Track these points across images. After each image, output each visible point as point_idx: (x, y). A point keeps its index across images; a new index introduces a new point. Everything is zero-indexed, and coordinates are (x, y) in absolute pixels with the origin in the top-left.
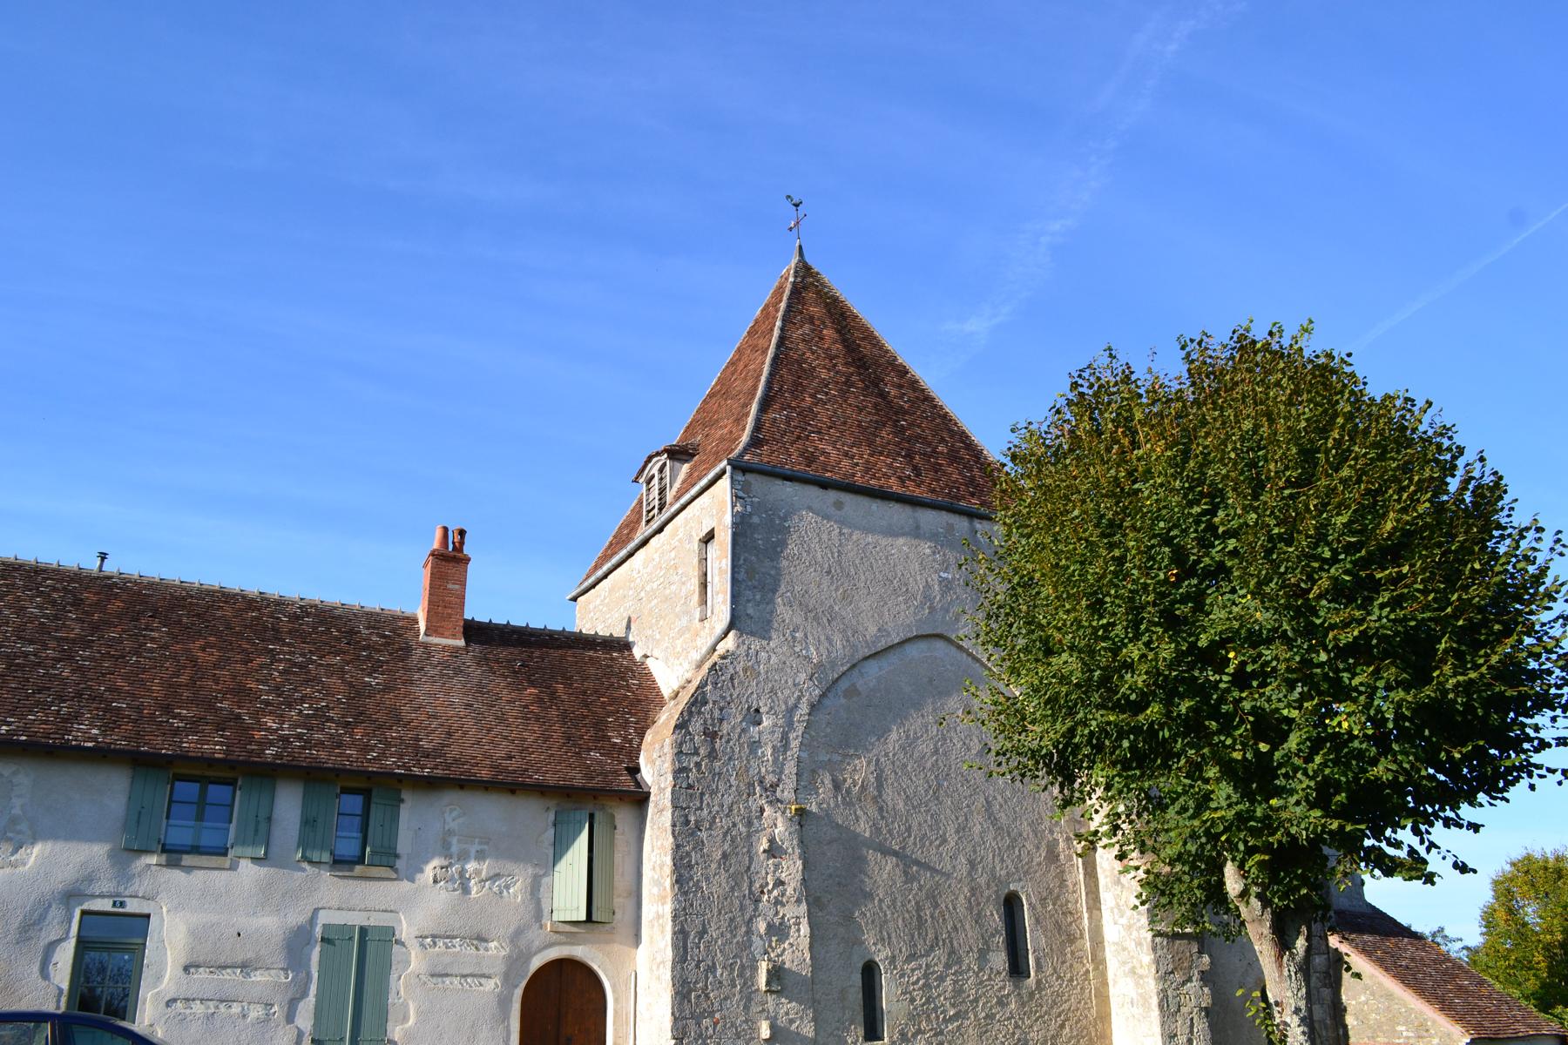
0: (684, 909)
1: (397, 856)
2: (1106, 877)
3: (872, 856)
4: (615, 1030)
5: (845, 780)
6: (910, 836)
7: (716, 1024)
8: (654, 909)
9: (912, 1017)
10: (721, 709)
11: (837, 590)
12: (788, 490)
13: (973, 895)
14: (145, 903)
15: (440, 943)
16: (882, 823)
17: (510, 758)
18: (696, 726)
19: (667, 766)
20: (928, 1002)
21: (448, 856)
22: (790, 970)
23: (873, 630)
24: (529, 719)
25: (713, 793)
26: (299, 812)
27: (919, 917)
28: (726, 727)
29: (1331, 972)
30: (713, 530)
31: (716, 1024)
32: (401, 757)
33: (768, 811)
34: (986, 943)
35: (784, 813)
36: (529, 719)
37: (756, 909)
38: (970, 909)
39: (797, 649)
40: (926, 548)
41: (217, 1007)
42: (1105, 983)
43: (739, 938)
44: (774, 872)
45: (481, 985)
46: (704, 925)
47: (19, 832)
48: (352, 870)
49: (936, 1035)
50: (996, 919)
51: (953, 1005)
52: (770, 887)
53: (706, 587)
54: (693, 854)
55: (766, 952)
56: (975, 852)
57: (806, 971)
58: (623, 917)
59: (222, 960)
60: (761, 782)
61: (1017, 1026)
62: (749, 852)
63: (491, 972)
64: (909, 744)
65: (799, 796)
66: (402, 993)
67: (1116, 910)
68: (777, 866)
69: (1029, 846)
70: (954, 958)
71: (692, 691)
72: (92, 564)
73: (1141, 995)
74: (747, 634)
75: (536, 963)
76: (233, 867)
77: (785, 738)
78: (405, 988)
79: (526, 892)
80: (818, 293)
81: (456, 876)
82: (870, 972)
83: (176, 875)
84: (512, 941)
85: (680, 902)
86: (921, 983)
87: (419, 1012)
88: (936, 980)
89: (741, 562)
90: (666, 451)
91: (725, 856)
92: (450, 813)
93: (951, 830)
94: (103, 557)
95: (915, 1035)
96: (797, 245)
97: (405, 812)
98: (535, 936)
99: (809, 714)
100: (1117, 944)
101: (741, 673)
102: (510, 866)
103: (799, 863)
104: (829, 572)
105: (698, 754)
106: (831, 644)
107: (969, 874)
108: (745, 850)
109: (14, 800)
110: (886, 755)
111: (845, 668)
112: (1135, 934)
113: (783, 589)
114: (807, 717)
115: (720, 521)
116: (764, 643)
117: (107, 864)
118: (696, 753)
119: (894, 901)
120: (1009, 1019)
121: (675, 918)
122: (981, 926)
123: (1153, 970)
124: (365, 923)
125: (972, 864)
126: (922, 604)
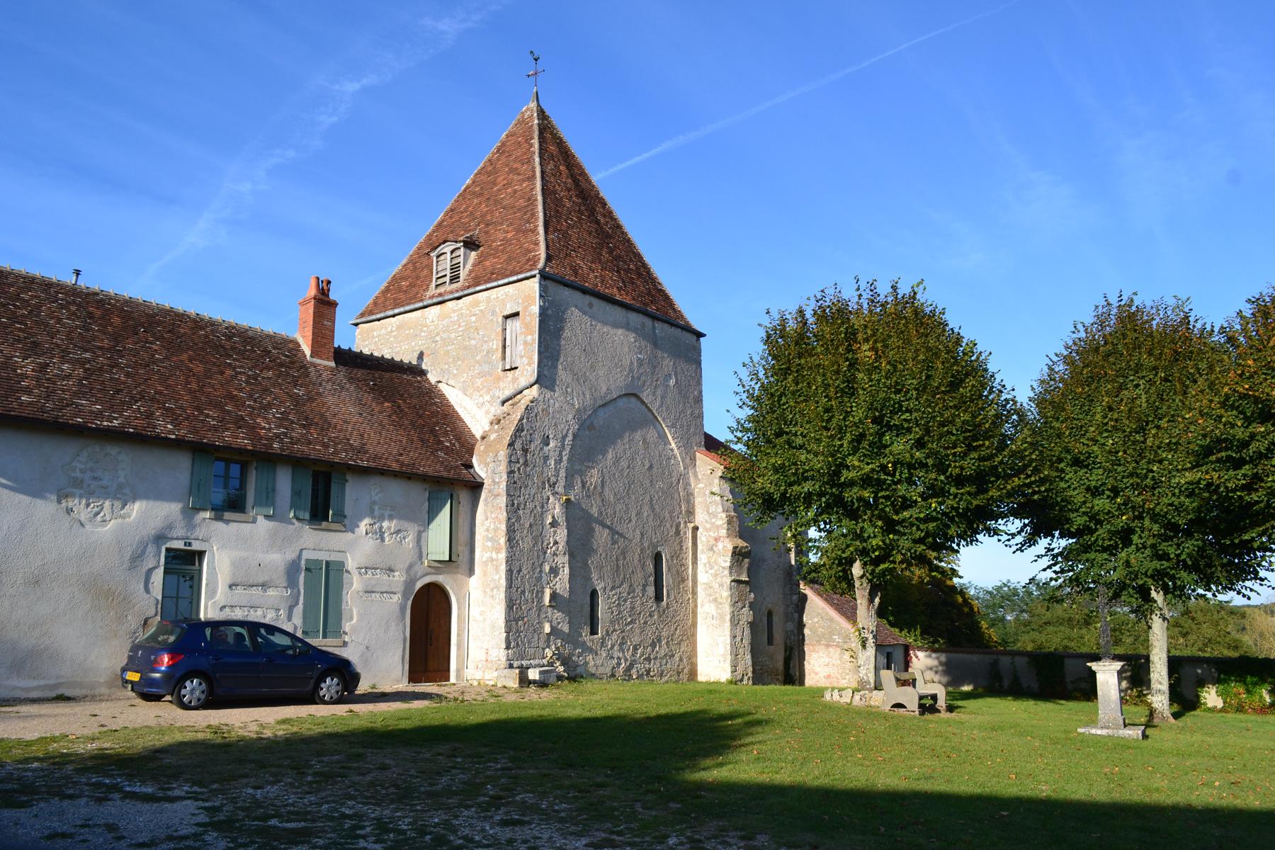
1: (345, 517)
3: (598, 528)
4: (458, 626)
7: (525, 624)
8: (488, 554)
9: (612, 622)
10: (531, 435)
11: (588, 362)
12: (566, 292)
14: (204, 543)
15: (369, 572)
16: (603, 509)
17: (401, 455)
18: (518, 445)
19: (503, 468)
20: (619, 614)
21: (373, 517)
22: (558, 594)
23: (604, 389)
25: (526, 486)
26: (290, 486)
27: (617, 565)
31: (525, 624)
32: (346, 451)
33: (551, 498)
34: (646, 581)
37: (544, 558)
38: (640, 561)
41: (249, 611)
42: (696, 606)
47: (125, 494)
48: (320, 525)
49: (622, 632)
50: (650, 568)
51: (630, 616)
55: (548, 583)
57: (566, 595)
58: (463, 558)
59: (251, 582)
61: (657, 629)
64: (617, 461)
66: (349, 603)
68: (555, 532)
69: (668, 526)
70: (631, 590)
71: (516, 422)
72: (70, 279)
73: (719, 613)
75: (419, 585)
76: (254, 521)
77: (560, 454)
82: (594, 594)
83: (220, 525)
87: (359, 615)
91: (531, 525)
93: (634, 515)
94: (78, 273)
95: (612, 632)
96: (535, 91)
97: (349, 488)
102: (405, 524)
103: (566, 531)
104: (585, 350)
107: (641, 541)
109: (119, 472)
112: (719, 580)
113: (561, 360)
116: (552, 393)
117: (180, 517)
118: (518, 462)
119: (607, 555)
120: (653, 624)
121: (507, 561)
122: (644, 571)
124: (328, 559)
125: (642, 534)
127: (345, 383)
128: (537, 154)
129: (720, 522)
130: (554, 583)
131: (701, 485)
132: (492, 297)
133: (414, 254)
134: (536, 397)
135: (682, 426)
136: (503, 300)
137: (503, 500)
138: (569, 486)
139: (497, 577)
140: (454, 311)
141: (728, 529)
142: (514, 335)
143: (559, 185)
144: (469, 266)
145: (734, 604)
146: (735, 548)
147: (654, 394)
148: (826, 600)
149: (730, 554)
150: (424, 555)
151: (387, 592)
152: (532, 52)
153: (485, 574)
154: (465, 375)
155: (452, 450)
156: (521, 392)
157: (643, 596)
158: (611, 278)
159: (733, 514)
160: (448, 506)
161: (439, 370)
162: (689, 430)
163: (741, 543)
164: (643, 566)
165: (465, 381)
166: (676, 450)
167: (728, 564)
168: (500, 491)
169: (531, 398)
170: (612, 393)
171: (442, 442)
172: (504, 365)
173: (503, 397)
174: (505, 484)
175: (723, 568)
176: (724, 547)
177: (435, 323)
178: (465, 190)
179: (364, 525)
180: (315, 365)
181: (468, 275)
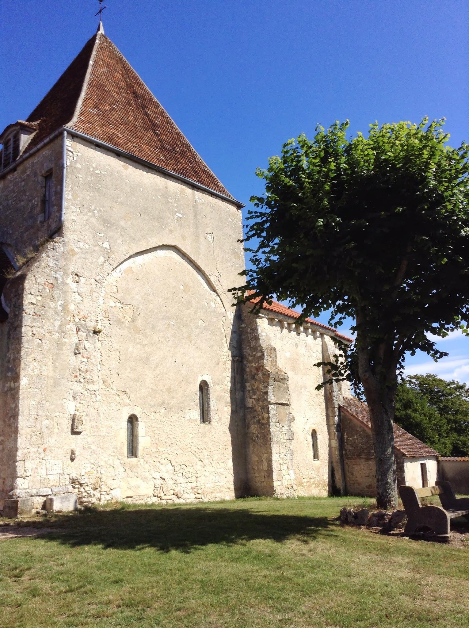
132: (35, 161)
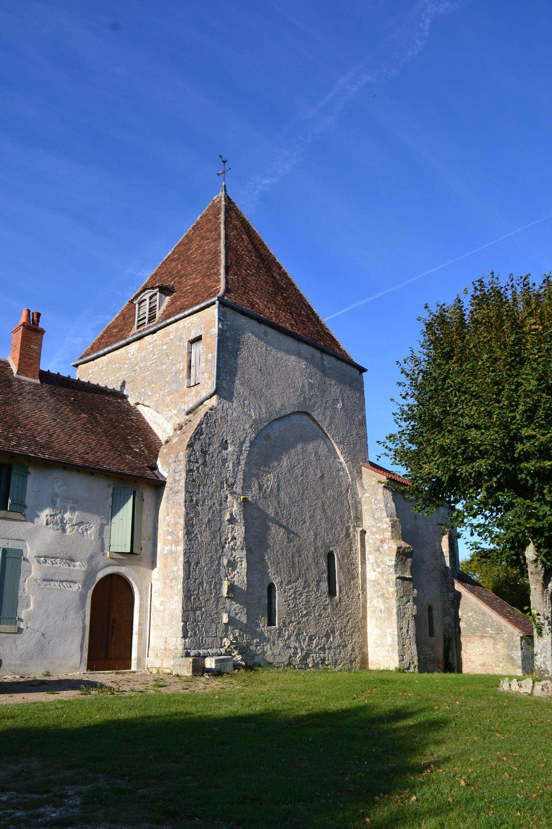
0: (189, 549)
1: (25, 507)
2: (370, 547)
3: (274, 528)
4: (140, 616)
5: (264, 485)
6: (290, 518)
7: (203, 614)
8: (167, 548)
9: (288, 614)
10: (210, 439)
11: (264, 380)
12: (243, 320)
13: (316, 552)
15: (49, 561)
16: (279, 510)
17: (88, 454)
19: (182, 467)
20: (295, 607)
22: (236, 586)
23: (279, 405)
24: (88, 432)
25: (205, 485)
27: (293, 561)
28: (211, 449)
29: (455, 600)
30: (201, 336)
31: (203, 614)
32: (29, 446)
33: (230, 498)
34: (320, 577)
35: (237, 500)
36: (88, 432)
37: (222, 552)
38: (314, 559)
39: (245, 410)
40: (303, 364)
42: (366, 601)
43: (214, 567)
44: (232, 532)
45: (71, 587)
46: (198, 559)
49: (298, 624)
50: (324, 565)
51: (305, 609)
52: (230, 540)
53: (190, 368)
54: (194, 518)
55: (226, 576)
56: (317, 529)
57: (244, 588)
58: (146, 551)
60: (227, 482)
61: (331, 621)
62: (220, 520)
63: (77, 579)
64: (291, 469)
65: (244, 491)
66: (26, 590)
67: (375, 564)
68: (233, 529)
69: (339, 529)
70: (306, 585)
71: (195, 426)
73: (387, 608)
74: (223, 398)
75: (100, 575)
77: (238, 458)
78: (28, 587)
79: (96, 534)
80: (236, 213)
81: (59, 522)
82: (271, 588)
84: (88, 562)
85: (187, 545)
86: (293, 596)
87: (36, 602)
88: (299, 595)
89: (221, 357)
90: (159, 287)
91: (209, 521)
92: (57, 483)
93: (308, 516)
95: (289, 623)
96: (223, 184)
98: (101, 560)
99: (250, 447)
100: (374, 581)
101: (219, 419)
102: (87, 516)
103: (243, 528)
104: (261, 370)
105: (198, 463)
106: (260, 409)
107: (314, 540)
108: (218, 519)
110: (282, 474)
111: (266, 424)
112: (385, 577)
113: (239, 376)
114: (248, 449)
115: (207, 332)
116: (231, 404)
120: (328, 617)
121: (185, 554)
122: (318, 568)
123: (395, 595)
124: (6, 547)
125: (316, 535)
126: (301, 395)
127: (46, 396)
128: (222, 223)
129: (385, 526)
130: (232, 575)
131: (367, 495)
132: (180, 327)
133: (125, 309)
134: (215, 405)
135: (349, 444)
136: (189, 327)
137: (181, 497)
138: (246, 487)
139: (176, 569)
140: (150, 344)
141: (392, 532)
142: (198, 357)
143: (241, 247)
144: (163, 307)
145: (400, 599)
146: (399, 548)
147: (324, 414)
148: (478, 596)
149: (395, 554)
150: (107, 546)
151: (66, 581)
152: (220, 156)
153: (165, 566)
154: (158, 395)
155: (141, 455)
156: (202, 403)
157: (317, 590)
158: (285, 316)
159: (396, 519)
160: (130, 502)
161: (137, 393)
162: (355, 447)
163: (404, 544)
164: (317, 564)
165: (157, 400)
166: (344, 464)
167: (393, 563)
168: (180, 488)
169: (210, 406)
170: (286, 409)
171: (132, 448)
172: (189, 382)
173: (187, 409)
174: (184, 481)
175: (389, 566)
176: (389, 547)
177: (136, 355)
178: (167, 259)
179: (45, 514)
180: (20, 381)
181: (162, 314)
